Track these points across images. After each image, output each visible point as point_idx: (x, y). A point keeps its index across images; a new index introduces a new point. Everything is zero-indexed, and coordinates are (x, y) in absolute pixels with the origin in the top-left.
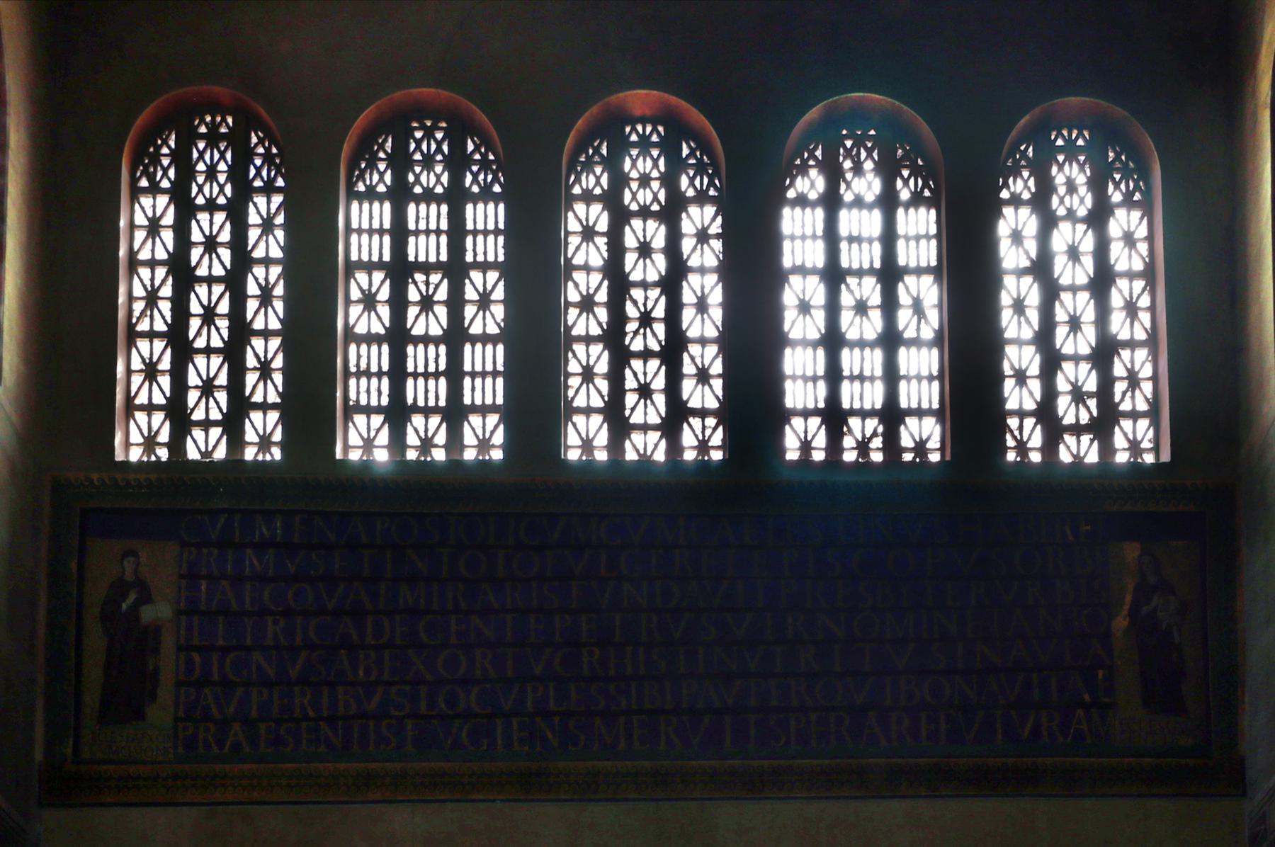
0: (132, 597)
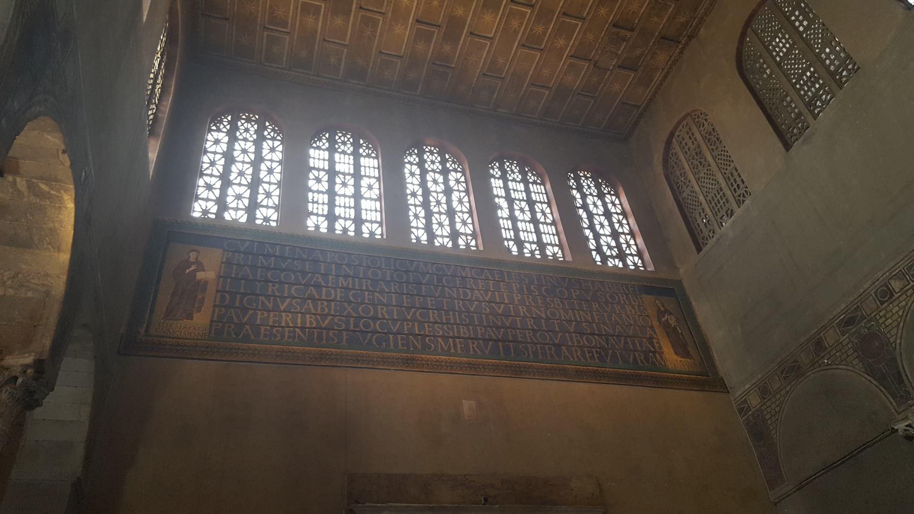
0: (193, 268)
